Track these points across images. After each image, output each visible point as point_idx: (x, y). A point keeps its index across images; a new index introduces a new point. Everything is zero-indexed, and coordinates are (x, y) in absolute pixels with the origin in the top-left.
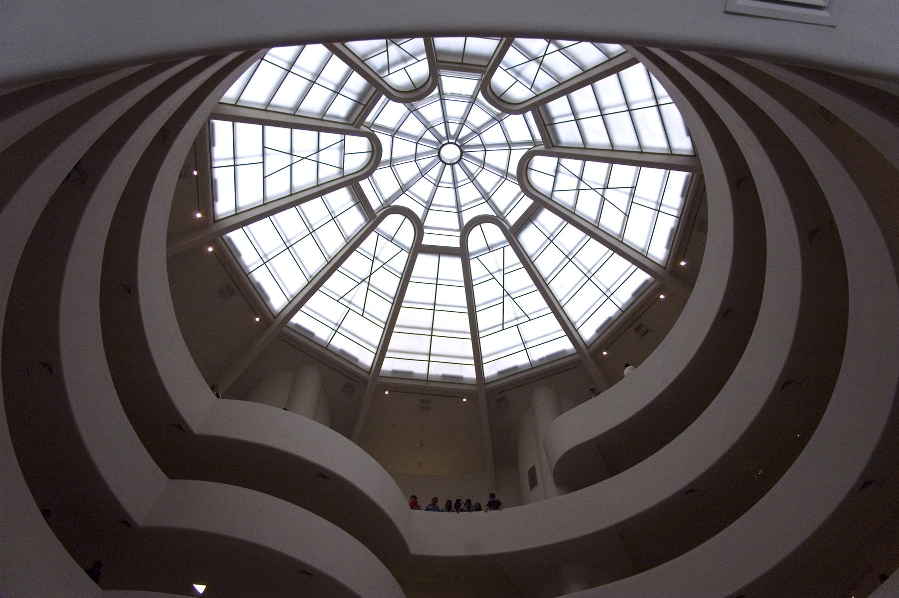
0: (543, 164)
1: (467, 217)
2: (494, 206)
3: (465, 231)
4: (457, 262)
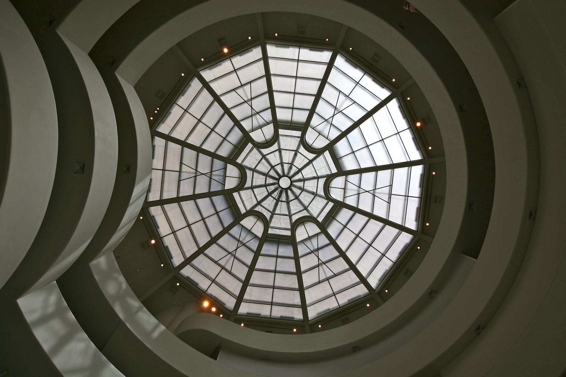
1: (311, 156)
3: (319, 152)
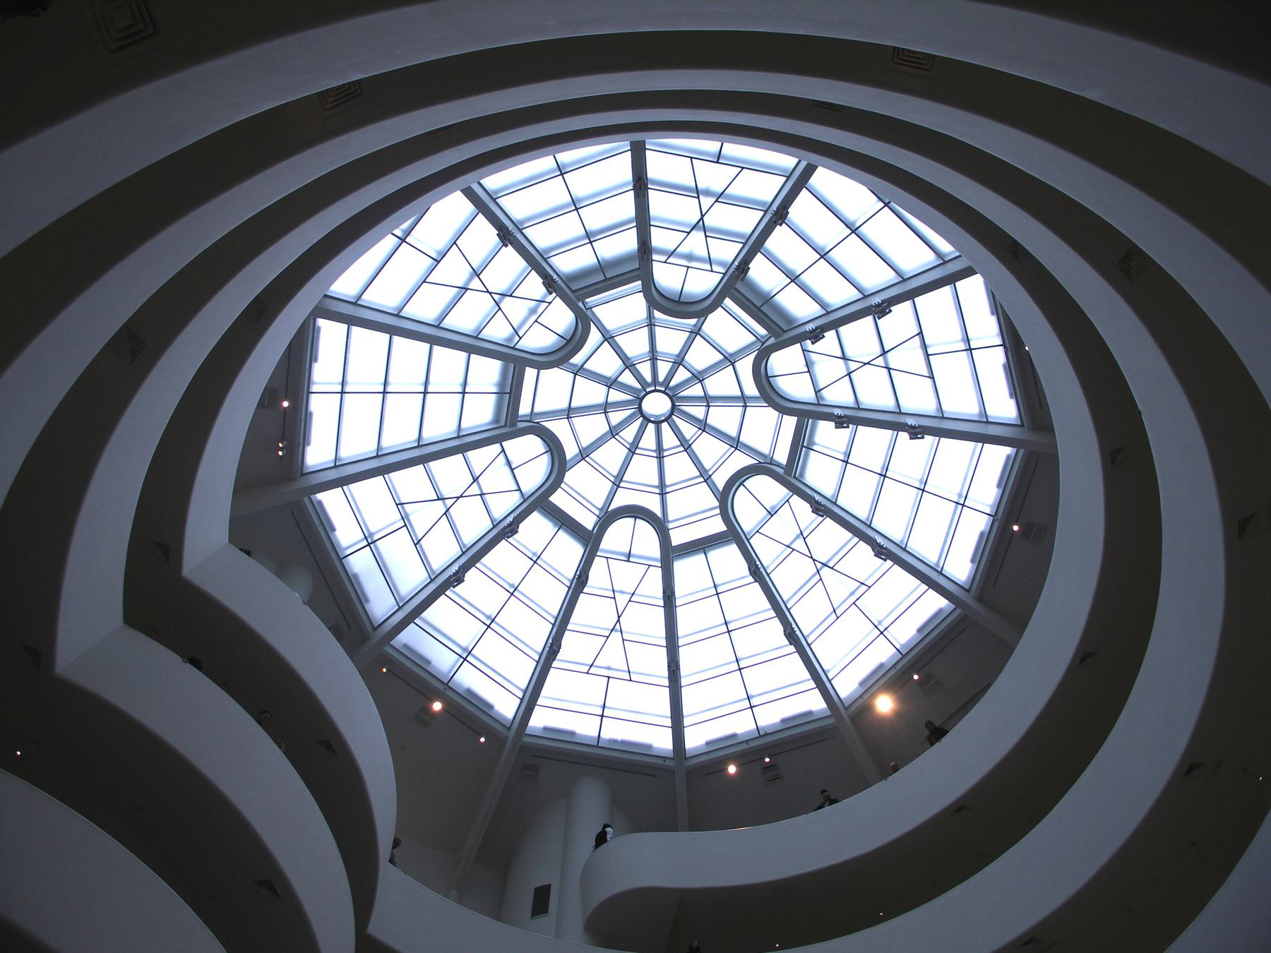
0: (785, 362)
1: (720, 480)
2: (749, 450)
4: (732, 550)
